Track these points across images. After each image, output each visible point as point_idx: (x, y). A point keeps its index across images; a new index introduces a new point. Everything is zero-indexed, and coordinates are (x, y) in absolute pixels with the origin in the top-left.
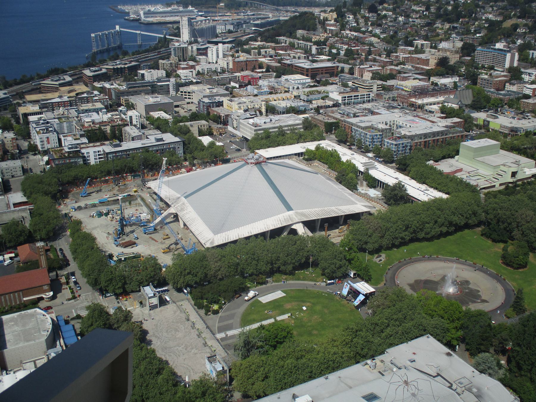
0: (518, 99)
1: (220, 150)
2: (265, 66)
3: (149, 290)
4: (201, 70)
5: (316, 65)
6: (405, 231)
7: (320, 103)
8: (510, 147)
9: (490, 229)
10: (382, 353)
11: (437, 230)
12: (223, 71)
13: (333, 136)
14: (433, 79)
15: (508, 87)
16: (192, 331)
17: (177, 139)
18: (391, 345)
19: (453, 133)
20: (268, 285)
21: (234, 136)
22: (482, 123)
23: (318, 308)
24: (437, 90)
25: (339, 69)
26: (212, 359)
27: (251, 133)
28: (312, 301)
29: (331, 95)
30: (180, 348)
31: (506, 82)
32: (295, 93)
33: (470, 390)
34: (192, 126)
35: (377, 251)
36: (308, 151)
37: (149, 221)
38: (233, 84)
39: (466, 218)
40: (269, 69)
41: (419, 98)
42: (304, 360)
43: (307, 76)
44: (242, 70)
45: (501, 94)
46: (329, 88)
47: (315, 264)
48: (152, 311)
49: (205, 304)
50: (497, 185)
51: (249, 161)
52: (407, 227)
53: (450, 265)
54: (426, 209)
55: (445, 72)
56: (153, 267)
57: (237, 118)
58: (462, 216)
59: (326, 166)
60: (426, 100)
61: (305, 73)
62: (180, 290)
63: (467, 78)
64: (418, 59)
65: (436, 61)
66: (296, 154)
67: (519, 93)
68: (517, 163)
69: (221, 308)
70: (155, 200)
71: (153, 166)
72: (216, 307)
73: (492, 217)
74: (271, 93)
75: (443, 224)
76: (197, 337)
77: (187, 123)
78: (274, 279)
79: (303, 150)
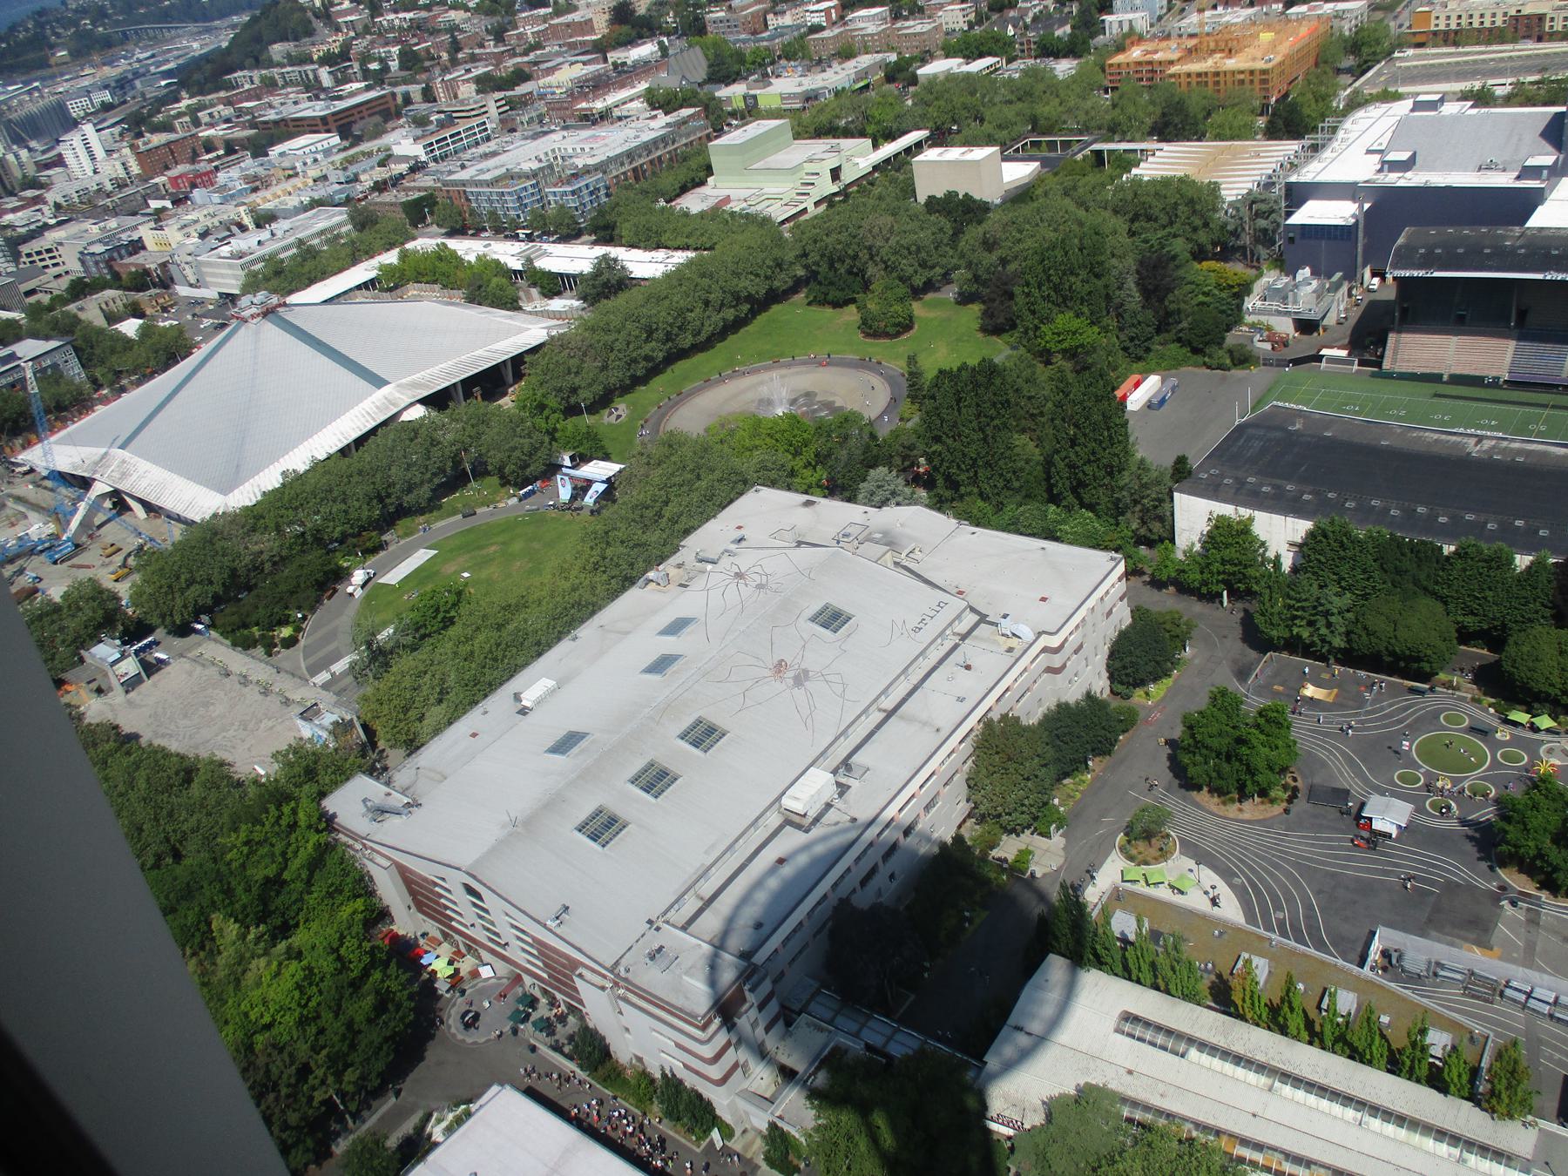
0: (802, 37)
1: (175, 334)
2: (219, 144)
3: (105, 651)
4: (60, 200)
5: (341, 105)
6: (647, 341)
7: (380, 174)
8: (811, 129)
9: (820, 283)
10: (676, 550)
11: (715, 320)
12: (120, 185)
13: (434, 228)
14: (613, 56)
15: (773, 21)
16: (246, 690)
17: (53, 344)
18: (687, 532)
19: (688, 135)
20: (391, 548)
21: (200, 302)
22: (742, 105)
23: (517, 546)
24: (625, 75)
25: (399, 100)
26: (309, 713)
27: (236, 277)
28: (500, 539)
29: (397, 150)
30: (231, 733)
31: (766, 12)
32: (314, 173)
33: (869, 539)
34: (81, 309)
35: (603, 401)
36: (387, 270)
37: (55, 537)
38: (154, 204)
39: (767, 278)
40: (231, 147)
41: (595, 98)
42: (511, 627)
43: (328, 131)
44: (167, 168)
45: (763, 40)
46: (388, 139)
47: (480, 471)
48: (132, 695)
49: (257, 634)
50: (811, 208)
51: (246, 314)
52: (650, 332)
53: (765, 376)
54: (675, 282)
55: (634, 34)
56: (93, 599)
57: (190, 259)
58: (757, 275)
59: (437, 287)
60: (612, 98)
61: (321, 128)
62: (184, 630)
63: (684, 34)
64: (568, 25)
65: (607, 17)
66: (359, 287)
67: (798, 27)
68: (833, 150)
69: (298, 630)
70: (52, 490)
71: (16, 421)
72: (286, 632)
73: (817, 258)
74: (255, 190)
75: (722, 305)
76: (261, 697)
77: (72, 307)
78: (400, 533)
79: (373, 274)
